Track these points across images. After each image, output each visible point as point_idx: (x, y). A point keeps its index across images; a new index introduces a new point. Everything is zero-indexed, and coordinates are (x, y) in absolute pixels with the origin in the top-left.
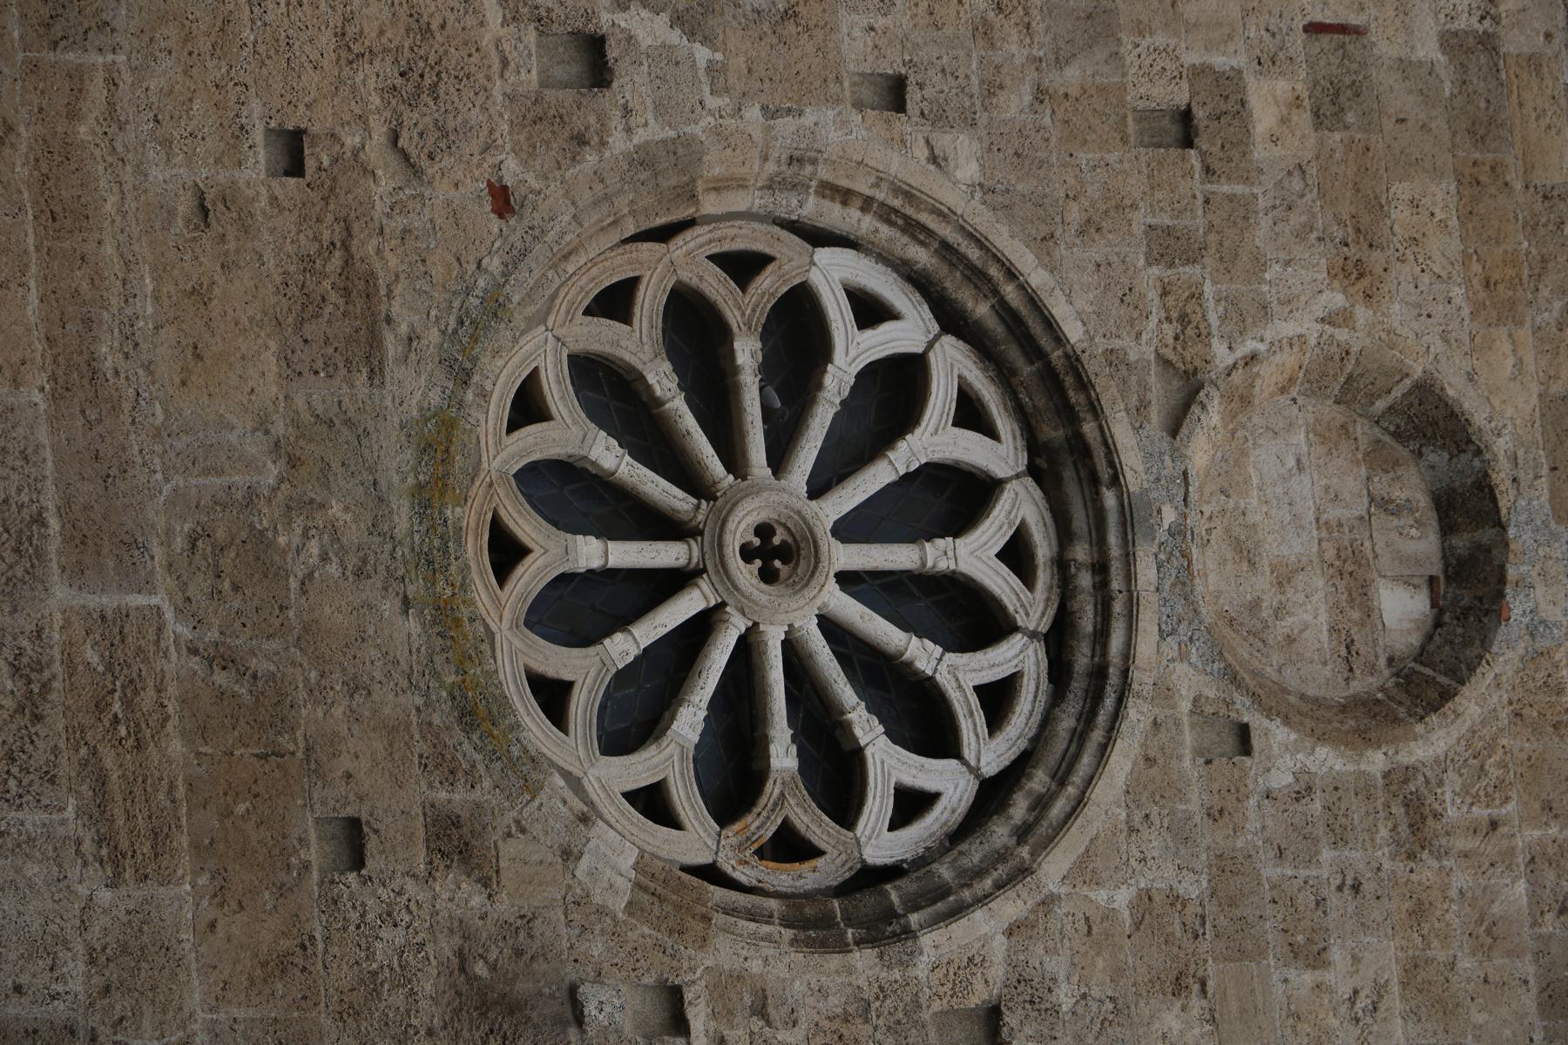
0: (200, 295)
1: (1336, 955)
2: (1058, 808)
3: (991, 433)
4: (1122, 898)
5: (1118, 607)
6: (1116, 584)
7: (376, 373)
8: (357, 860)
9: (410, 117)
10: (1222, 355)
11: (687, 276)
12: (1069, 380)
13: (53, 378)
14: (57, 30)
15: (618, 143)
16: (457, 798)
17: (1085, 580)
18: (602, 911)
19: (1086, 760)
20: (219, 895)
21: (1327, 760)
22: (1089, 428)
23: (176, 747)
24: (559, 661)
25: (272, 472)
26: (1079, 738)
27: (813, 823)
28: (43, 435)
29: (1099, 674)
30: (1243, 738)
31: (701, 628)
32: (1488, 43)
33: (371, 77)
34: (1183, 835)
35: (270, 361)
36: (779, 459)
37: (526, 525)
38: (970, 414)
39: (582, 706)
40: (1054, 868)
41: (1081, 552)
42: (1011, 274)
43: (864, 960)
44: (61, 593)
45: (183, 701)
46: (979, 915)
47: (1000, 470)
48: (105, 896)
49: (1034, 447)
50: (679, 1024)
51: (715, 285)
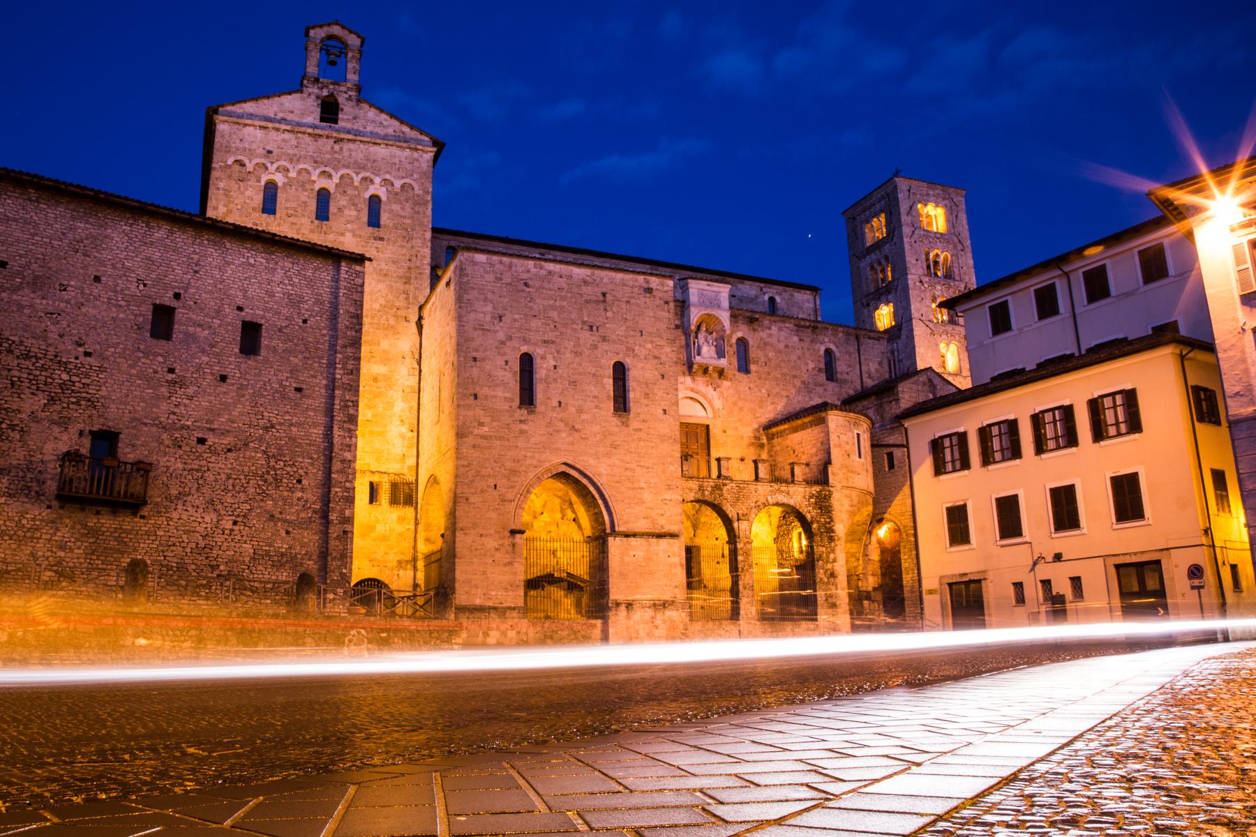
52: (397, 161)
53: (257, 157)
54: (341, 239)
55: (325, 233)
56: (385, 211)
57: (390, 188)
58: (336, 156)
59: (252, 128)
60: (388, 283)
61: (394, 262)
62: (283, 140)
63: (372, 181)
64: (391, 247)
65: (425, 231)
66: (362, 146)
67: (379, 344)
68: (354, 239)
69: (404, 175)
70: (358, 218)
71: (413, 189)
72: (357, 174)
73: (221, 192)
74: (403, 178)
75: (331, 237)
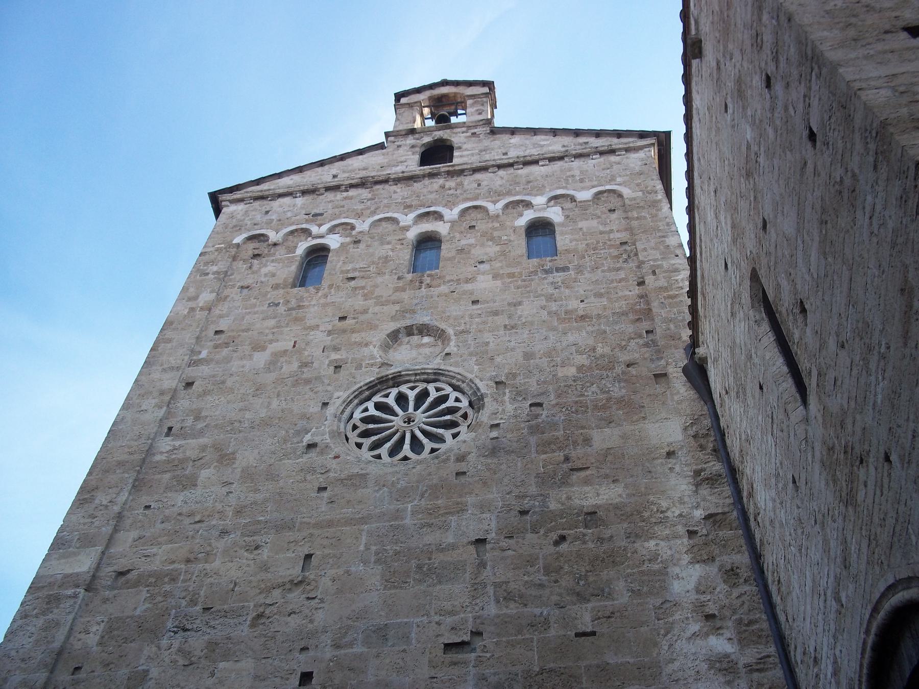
0: (349, 502)
1: (487, 341)
2: (459, 377)
3: (390, 393)
4: (475, 367)
5: (423, 371)
6: (419, 372)
7: (367, 474)
8: (464, 473)
9: (318, 471)
10: (380, 360)
11: (356, 435)
12: (381, 380)
13: (363, 524)
14: (292, 527)
15: (328, 441)
16: (452, 458)
17: (418, 377)
18: (476, 436)
19: (451, 374)
20: (471, 493)
21: (452, 343)
22: (390, 376)
23: (440, 502)
24: (427, 449)
25: (385, 489)
26: (446, 376)
27: (461, 413)
28: (374, 525)
29: (435, 374)
30: (447, 354)
31: (424, 432)
32: (329, 331)
33: (309, 477)
34: (464, 361)
35: (363, 490)
36: (391, 421)
37: (401, 455)
38: (387, 396)
39: (436, 446)
40: (470, 376)
41: (413, 378)
42: (361, 387)
43: (486, 400)
44: (408, 521)
45: (430, 501)
46: (478, 385)
47: (397, 391)
48: (469, 512)
49: (394, 387)
50: (498, 425)
51: (358, 431)
52: (577, 173)
53: (291, 225)
54: (469, 287)
55: (429, 286)
56: (562, 234)
57: (568, 205)
58: (451, 192)
59: (287, 200)
60: (590, 329)
61: (599, 295)
62: (345, 198)
63: (528, 205)
64: (587, 275)
65: (663, 237)
66: (501, 173)
67: (587, 441)
68: (499, 283)
69: (596, 183)
70: (503, 253)
71: (620, 196)
72: (495, 202)
73: (211, 276)
74: (593, 187)
75: (444, 289)
